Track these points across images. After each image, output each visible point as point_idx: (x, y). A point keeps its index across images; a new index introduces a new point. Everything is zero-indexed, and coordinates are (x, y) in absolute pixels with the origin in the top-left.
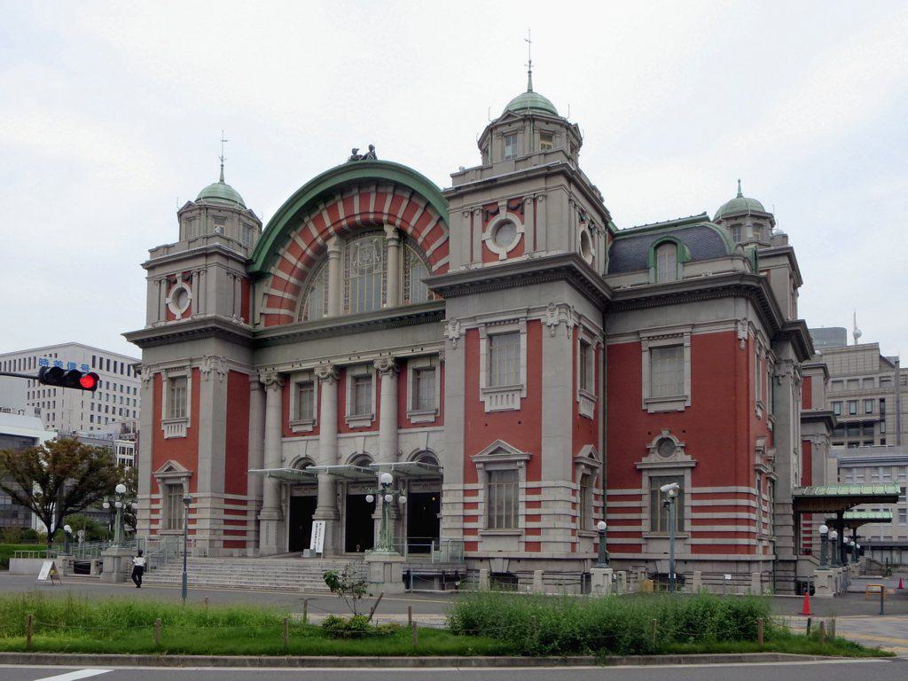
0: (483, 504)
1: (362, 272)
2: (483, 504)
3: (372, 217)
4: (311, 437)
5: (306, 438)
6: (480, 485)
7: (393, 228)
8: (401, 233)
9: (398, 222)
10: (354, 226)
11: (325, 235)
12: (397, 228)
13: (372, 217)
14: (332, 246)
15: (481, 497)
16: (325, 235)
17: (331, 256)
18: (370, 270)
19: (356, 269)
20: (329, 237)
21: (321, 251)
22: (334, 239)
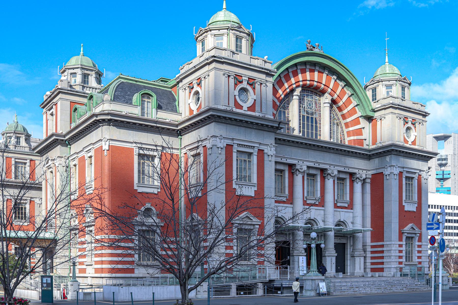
0: (404, 251)
1: (307, 113)
2: (404, 251)
3: (323, 86)
4: (285, 205)
6: (404, 243)
7: (331, 98)
8: (334, 102)
9: (335, 97)
10: (311, 86)
11: (297, 84)
12: (332, 99)
13: (323, 86)
14: (298, 92)
15: (404, 248)
16: (297, 84)
17: (294, 97)
18: (312, 114)
19: (305, 110)
20: (298, 87)
21: (292, 91)
22: (299, 89)
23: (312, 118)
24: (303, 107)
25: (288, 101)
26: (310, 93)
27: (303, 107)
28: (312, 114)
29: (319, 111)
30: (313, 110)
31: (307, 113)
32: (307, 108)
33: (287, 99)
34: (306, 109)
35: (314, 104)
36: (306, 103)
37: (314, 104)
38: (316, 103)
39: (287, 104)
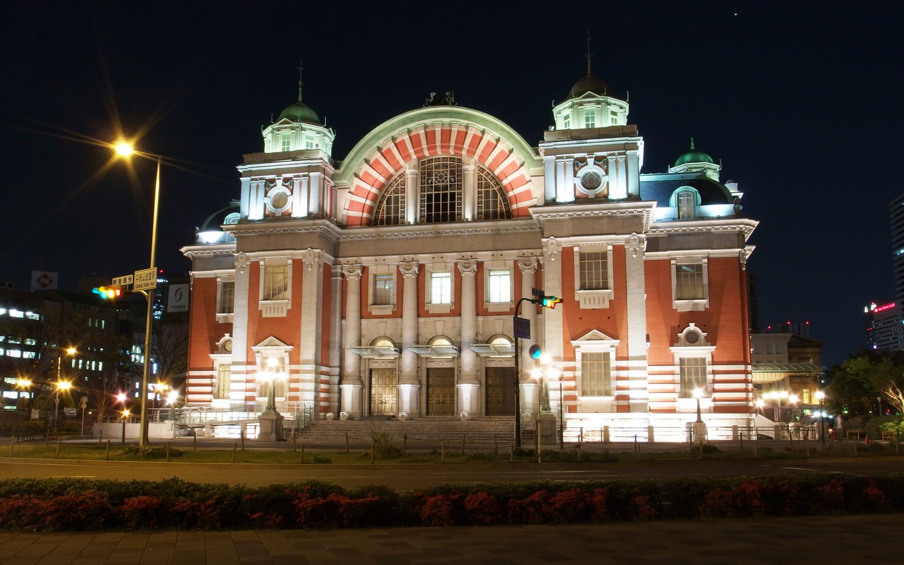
5: (385, 320)
23: (445, 195)
24: (429, 183)
25: (403, 181)
26: (443, 161)
27: (429, 183)
28: (445, 188)
29: (458, 181)
30: (447, 182)
31: (437, 188)
32: (435, 183)
33: (402, 179)
34: (433, 185)
35: (448, 175)
36: (434, 175)
37: (448, 175)
38: (452, 173)
39: (401, 185)
